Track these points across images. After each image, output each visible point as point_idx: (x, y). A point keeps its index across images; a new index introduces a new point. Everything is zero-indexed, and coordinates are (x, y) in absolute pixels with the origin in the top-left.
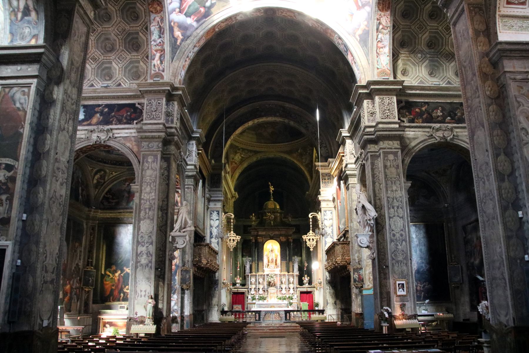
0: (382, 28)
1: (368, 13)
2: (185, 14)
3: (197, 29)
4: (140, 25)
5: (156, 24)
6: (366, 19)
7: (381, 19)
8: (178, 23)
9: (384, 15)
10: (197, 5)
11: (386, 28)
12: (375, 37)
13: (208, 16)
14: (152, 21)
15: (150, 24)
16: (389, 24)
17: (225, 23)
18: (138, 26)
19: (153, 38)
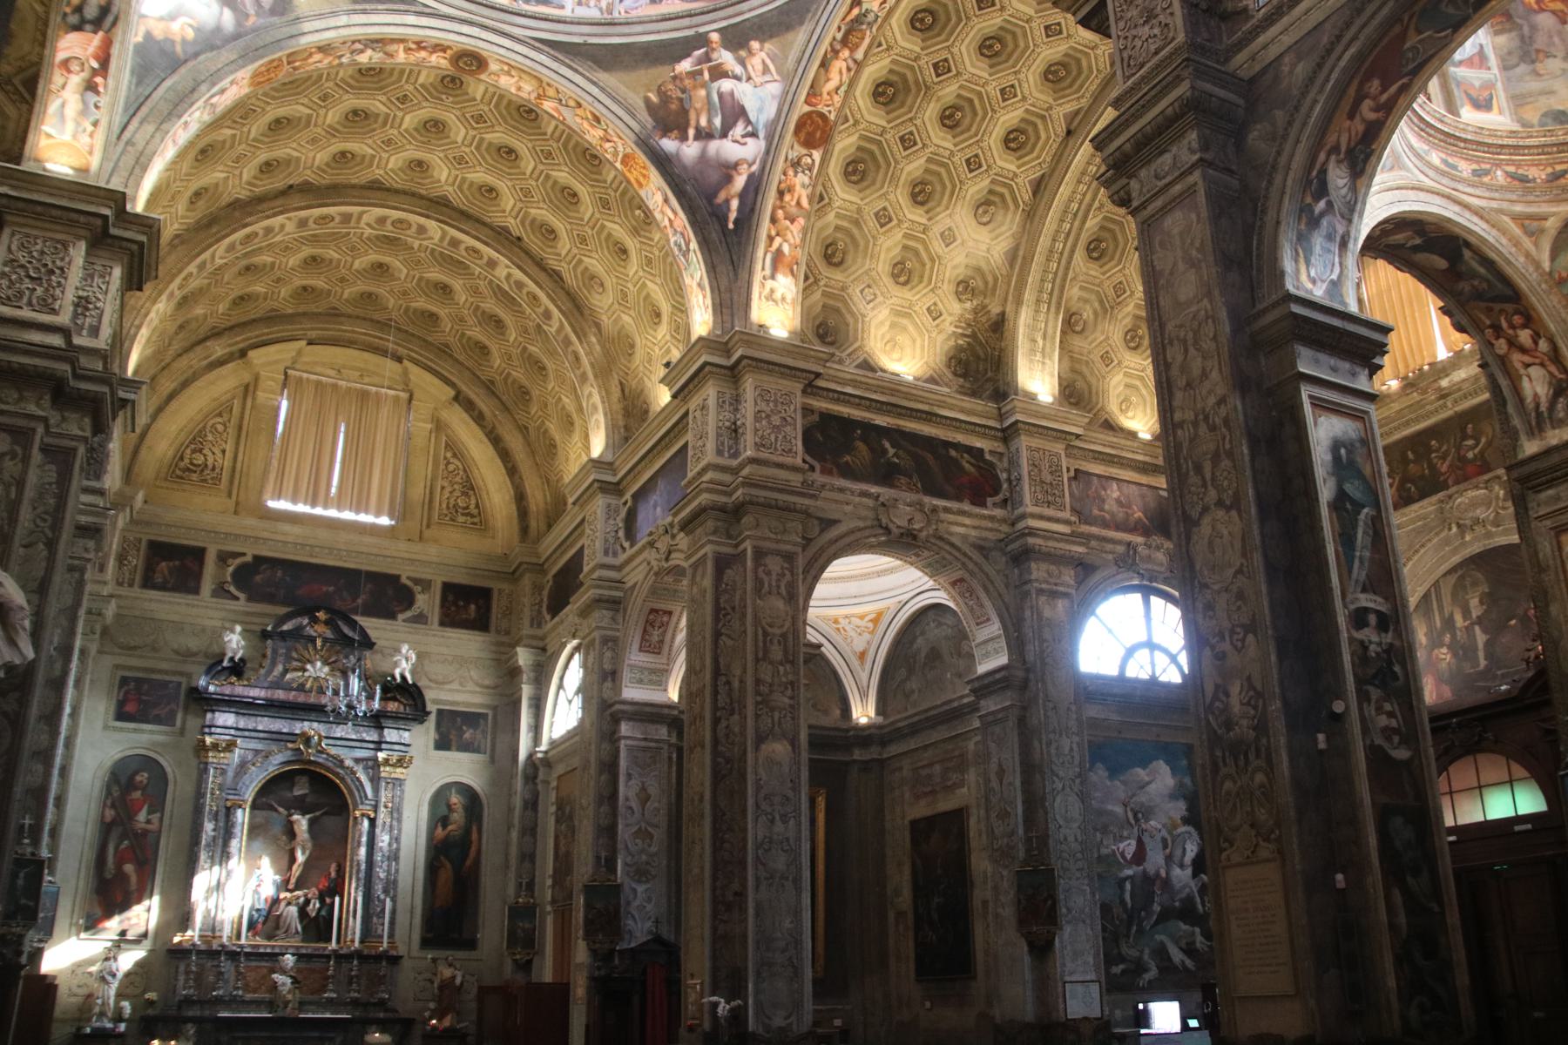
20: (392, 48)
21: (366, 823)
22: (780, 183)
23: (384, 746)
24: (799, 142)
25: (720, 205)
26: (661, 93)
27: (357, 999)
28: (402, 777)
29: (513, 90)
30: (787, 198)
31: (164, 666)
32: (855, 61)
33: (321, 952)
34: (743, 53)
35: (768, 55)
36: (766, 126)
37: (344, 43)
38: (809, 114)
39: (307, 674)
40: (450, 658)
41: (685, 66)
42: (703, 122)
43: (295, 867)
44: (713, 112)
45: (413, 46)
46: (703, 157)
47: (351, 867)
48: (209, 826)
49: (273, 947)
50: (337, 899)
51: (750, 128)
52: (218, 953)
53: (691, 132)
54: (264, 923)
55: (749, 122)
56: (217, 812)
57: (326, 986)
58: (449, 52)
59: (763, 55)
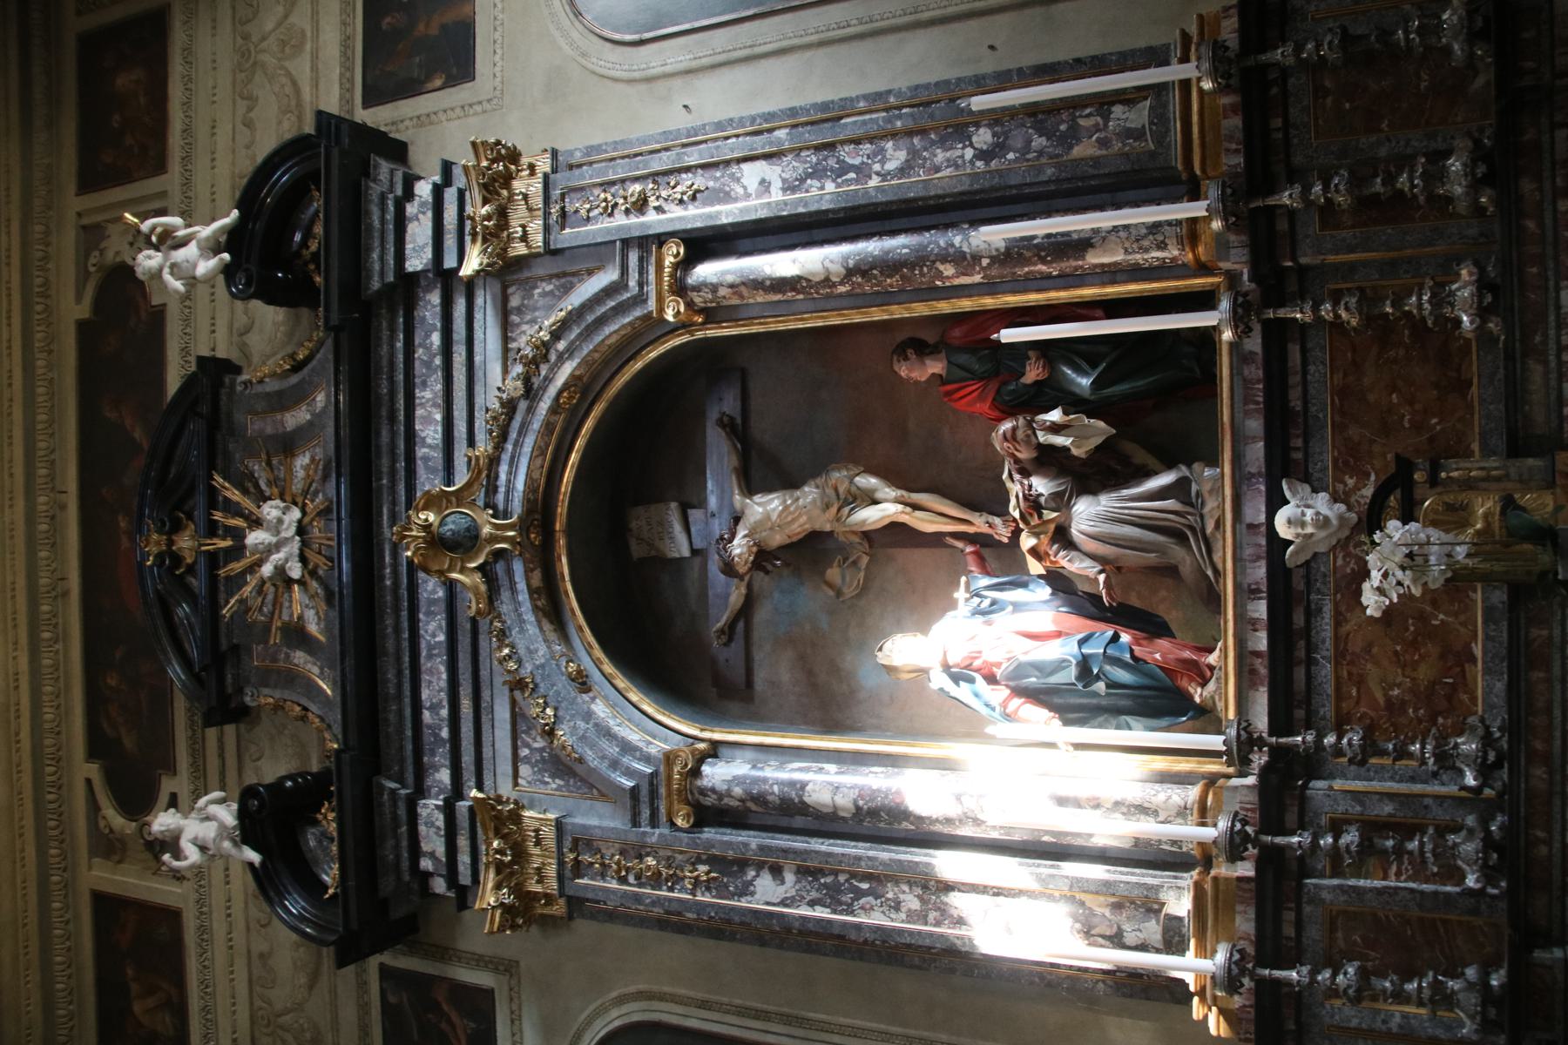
21: (706, 271)
23: (450, 262)
27: (1478, 154)
28: (544, 165)
31: (348, 1013)
33: (1255, 372)
39: (295, 571)
40: (242, 105)
43: (925, 523)
47: (885, 299)
48: (766, 894)
49: (1245, 593)
50: (1009, 335)
52: (1271, 860)
54: (1150, 626)
56: (714, 861)
57: (1416, 324)
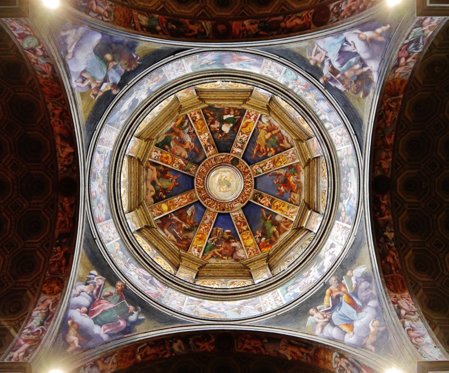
0: (406, 314)
1: (376, 309)
2: (94, 319)
3: (107, 343)
4: (18, 319)
5: (44, 308)
6: (375, 318)
7: (399, 302)
8: (79, 325)
9: (402, 297)
10: (115, 315)
11: (412, 313)
12: (401, 325)
13: (130, 332)
14: (39, 303)
15: (34, 308)
16: (414, 308)
17: (153, 351)
18: (13, 321)
19: (29, 325)
20: (381, 223)
22: (349, 17)
24: (328, 19)
25: (385, 37)
26: (357, 92)
29: (390, 160)
30: (354, 8)
32: (284, 18)
34: (319, 65)
35: (311, 55)
36: (338, 38)
37: (379, 247)
38: (314, 24)
41: (340, 87)
42: (358, 66)
44: (352, 65)
45: (378, 213)
46: (372, 58)
51: (345, 44)
53: (365, 69)
55: (342, 46)
58: (377, 196)
59: (313, 57)
